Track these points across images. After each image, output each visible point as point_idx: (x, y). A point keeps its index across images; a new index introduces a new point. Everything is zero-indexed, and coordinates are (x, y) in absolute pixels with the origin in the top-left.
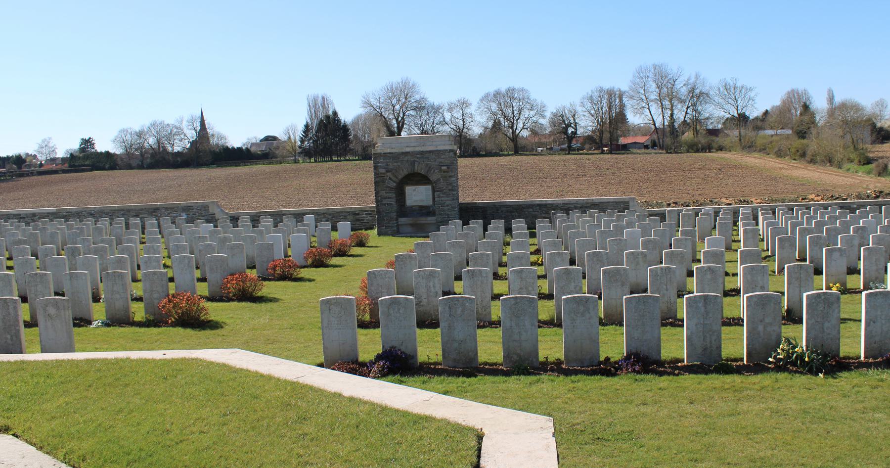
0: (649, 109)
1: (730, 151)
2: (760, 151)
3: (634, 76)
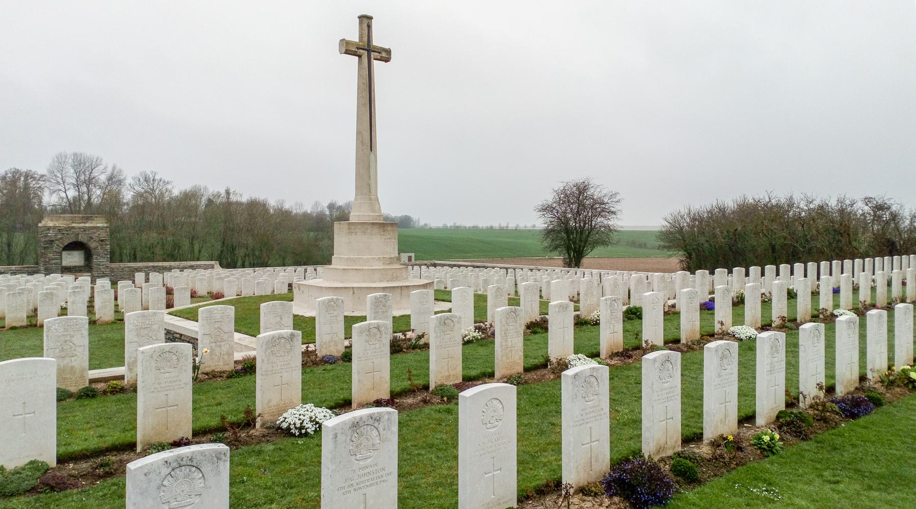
0: (65, 192)
3: (53, 161)
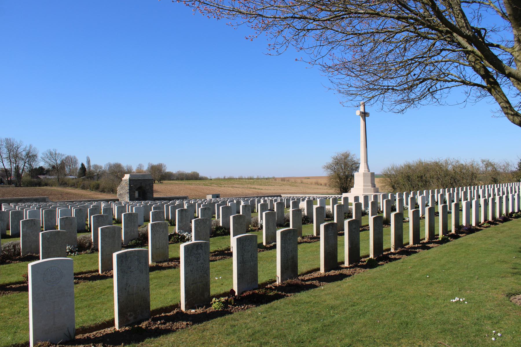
1: (52, 186)
2: (71, 186)
